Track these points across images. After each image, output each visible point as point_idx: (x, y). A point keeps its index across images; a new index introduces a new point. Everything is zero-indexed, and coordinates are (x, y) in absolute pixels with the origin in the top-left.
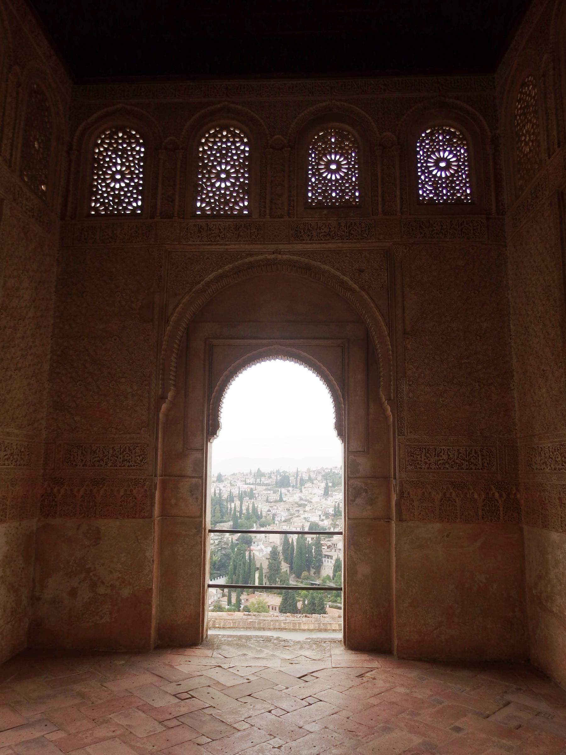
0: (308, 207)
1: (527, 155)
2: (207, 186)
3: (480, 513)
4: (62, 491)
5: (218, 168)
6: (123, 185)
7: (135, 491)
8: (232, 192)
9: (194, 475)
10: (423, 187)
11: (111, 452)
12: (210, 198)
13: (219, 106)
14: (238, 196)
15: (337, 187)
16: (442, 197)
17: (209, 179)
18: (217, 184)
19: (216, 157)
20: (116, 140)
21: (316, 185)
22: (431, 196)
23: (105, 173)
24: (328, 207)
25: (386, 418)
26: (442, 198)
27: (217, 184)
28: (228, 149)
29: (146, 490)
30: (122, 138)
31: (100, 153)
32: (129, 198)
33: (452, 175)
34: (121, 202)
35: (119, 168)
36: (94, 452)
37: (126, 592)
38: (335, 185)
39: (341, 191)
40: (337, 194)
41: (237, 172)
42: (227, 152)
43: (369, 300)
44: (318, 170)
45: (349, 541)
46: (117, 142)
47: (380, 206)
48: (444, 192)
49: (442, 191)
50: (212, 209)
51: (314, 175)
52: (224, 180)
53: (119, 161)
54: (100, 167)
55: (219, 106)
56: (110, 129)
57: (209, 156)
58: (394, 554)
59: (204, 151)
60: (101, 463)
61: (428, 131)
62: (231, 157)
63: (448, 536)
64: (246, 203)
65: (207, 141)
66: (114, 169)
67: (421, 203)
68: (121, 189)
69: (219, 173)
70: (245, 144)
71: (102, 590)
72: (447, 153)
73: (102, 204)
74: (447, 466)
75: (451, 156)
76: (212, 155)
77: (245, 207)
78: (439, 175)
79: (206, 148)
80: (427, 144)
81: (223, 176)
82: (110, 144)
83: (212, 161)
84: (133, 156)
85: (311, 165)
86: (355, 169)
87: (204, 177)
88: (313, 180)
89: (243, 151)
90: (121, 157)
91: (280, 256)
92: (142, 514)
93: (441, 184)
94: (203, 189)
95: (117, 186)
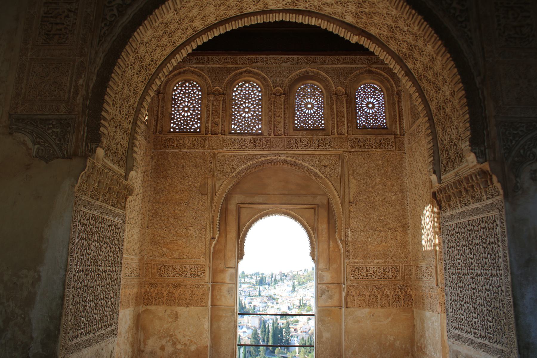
0: (295, 129)
2: (238, 116)
3: (391, 302)
4: (156, 291)
5: (244, 105)
6: (189, 114)
7: (197, 292)
8: (252, 120)
9: (230, 282)
11: (184, 269)
12: (239, 123)
13: (244, 69)
14: (255, 122)
15: (311, 118)
16: (370, 124)
17: (239, 112)
18: (243, 115)
19: (242, 99)
20: (185, 88)
21: (300, 116)
23: (178, 107)
24: (306, 130)
25: (339, 250)
27: (243, 115)
28: (249, 94)
29: (204, 291)
30: (188, 86)
31: (176, 95)
32: (192, 122)
33: (376, 112)
34: (187, 125)
35: (186, 104)
36: (174, 269)
37: (193, 348)
38: (310, 117)
39: (314, 120)
40: (312, 122)
41: (255, 108)
42: (249, 97)
43: (330, 183)
44: (301, 108)
45: (318, 319)
46: (185, 89)
47: (336, 130)
48: (371, 121)
49: (370, 121)
50: (241, 130)
52: (247, 113)
53: (187, 100)
54: (176, 103)
55: (244, 69)
56: (181, 81)
57: (239, 98)
58: (343, 326)
59: (236, 96)
60: (178, 275)
61: (362, 86)
62: (251, 99)
63: (373, 315)
64: (260, 126)
65: (237, 89)
66: (184, 105)
67: (358, 128)
68: (188, 116)
69: (244, 108)
70: (259, 92)
71: (179, 347)
72: (373, 99)
73: (177, 125)
74: (373, 277)
75: (375, 101)
76: (240, 97)
77: (260, 129)
78: (368, 111)
79: (237, 93)
80: (362, 94)
81: (247, 110)
82: (181, 90)
83: (241, 101)
84: (195, 97)
85: (297, 105)
86: (322, 107)
87: (235, 110)
88: (298, 113)
89: (258, 96)
90: (188, 97)
91: (279, 158)
92: (202, 304)
93: (369, 117)
94: (235, 117)
95: (186, 115)
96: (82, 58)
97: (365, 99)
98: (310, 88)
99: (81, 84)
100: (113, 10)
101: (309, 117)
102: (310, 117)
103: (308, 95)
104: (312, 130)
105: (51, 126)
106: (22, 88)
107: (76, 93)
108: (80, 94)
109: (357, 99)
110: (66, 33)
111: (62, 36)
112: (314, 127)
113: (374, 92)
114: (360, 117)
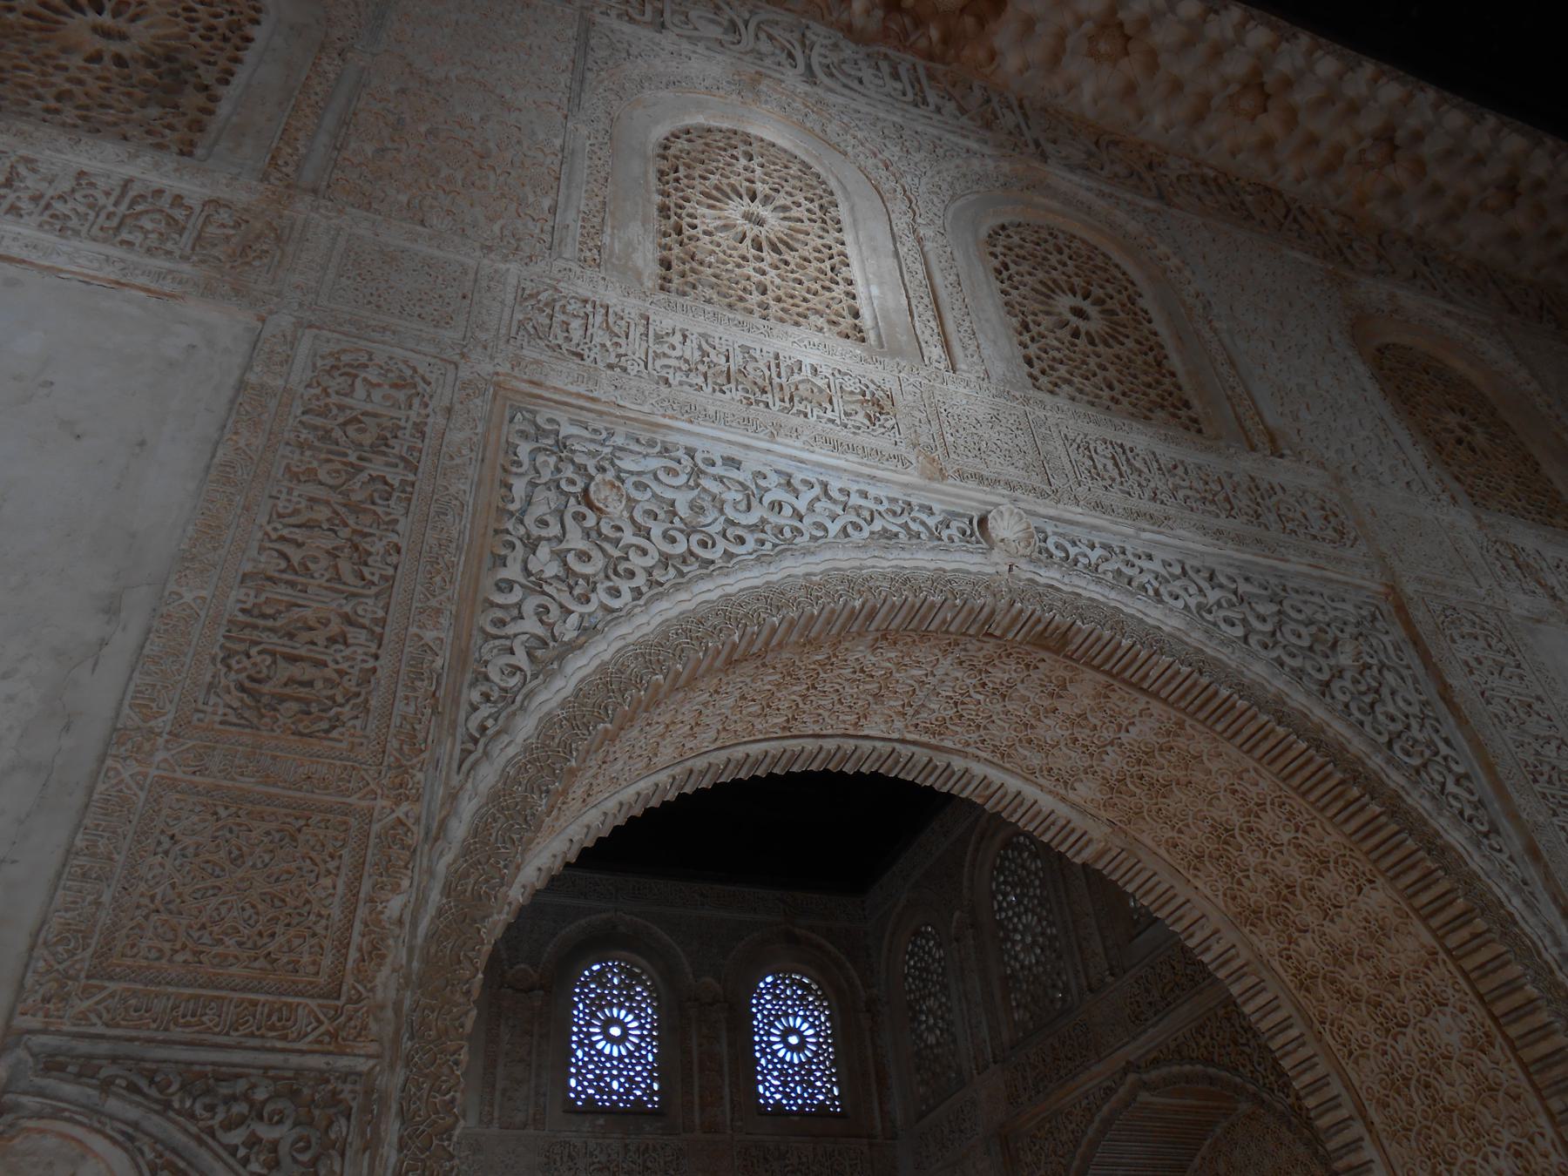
0: (570, 1108)
1: (931, 1047)
10: (765, 1080)
16: (795, 1099)
21: (585, 1064)
22: (778, 1096)
26: (796, 1104)
33: (810, 1061)
39: (629, 1079)
40: (621, 1085)
47: (697, 1114)
49: (794, 1090)
51: (580, 1044)
61: (769, 979)
67: (761, 1110)
72: (799, 1020)
75: (806, 1026)
78: (788, 1058)
80: (768, 1002)
88: (580, 1054)
93: (792, 1076)
96: (405, 807)
97: (778, 1018)
98: (619, 974)
99: (396, 914)
100: (513, 653)
101: (614, 1067)
102: (617, 1067)
103: (614, 996)
104: (624, 1112)
105: (240, 1108)
106: (98, 904)
107: (375, 953)
108: (389, 960)
109: (754, 1016)
110: (332, 698)
111: (314, 708)
112: (628, 1101)
113: (802, 998)
114: (764, 1076)
